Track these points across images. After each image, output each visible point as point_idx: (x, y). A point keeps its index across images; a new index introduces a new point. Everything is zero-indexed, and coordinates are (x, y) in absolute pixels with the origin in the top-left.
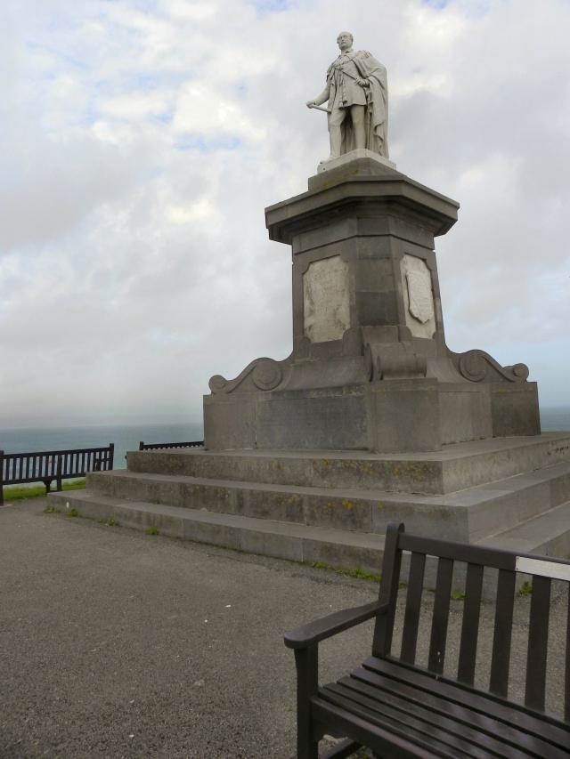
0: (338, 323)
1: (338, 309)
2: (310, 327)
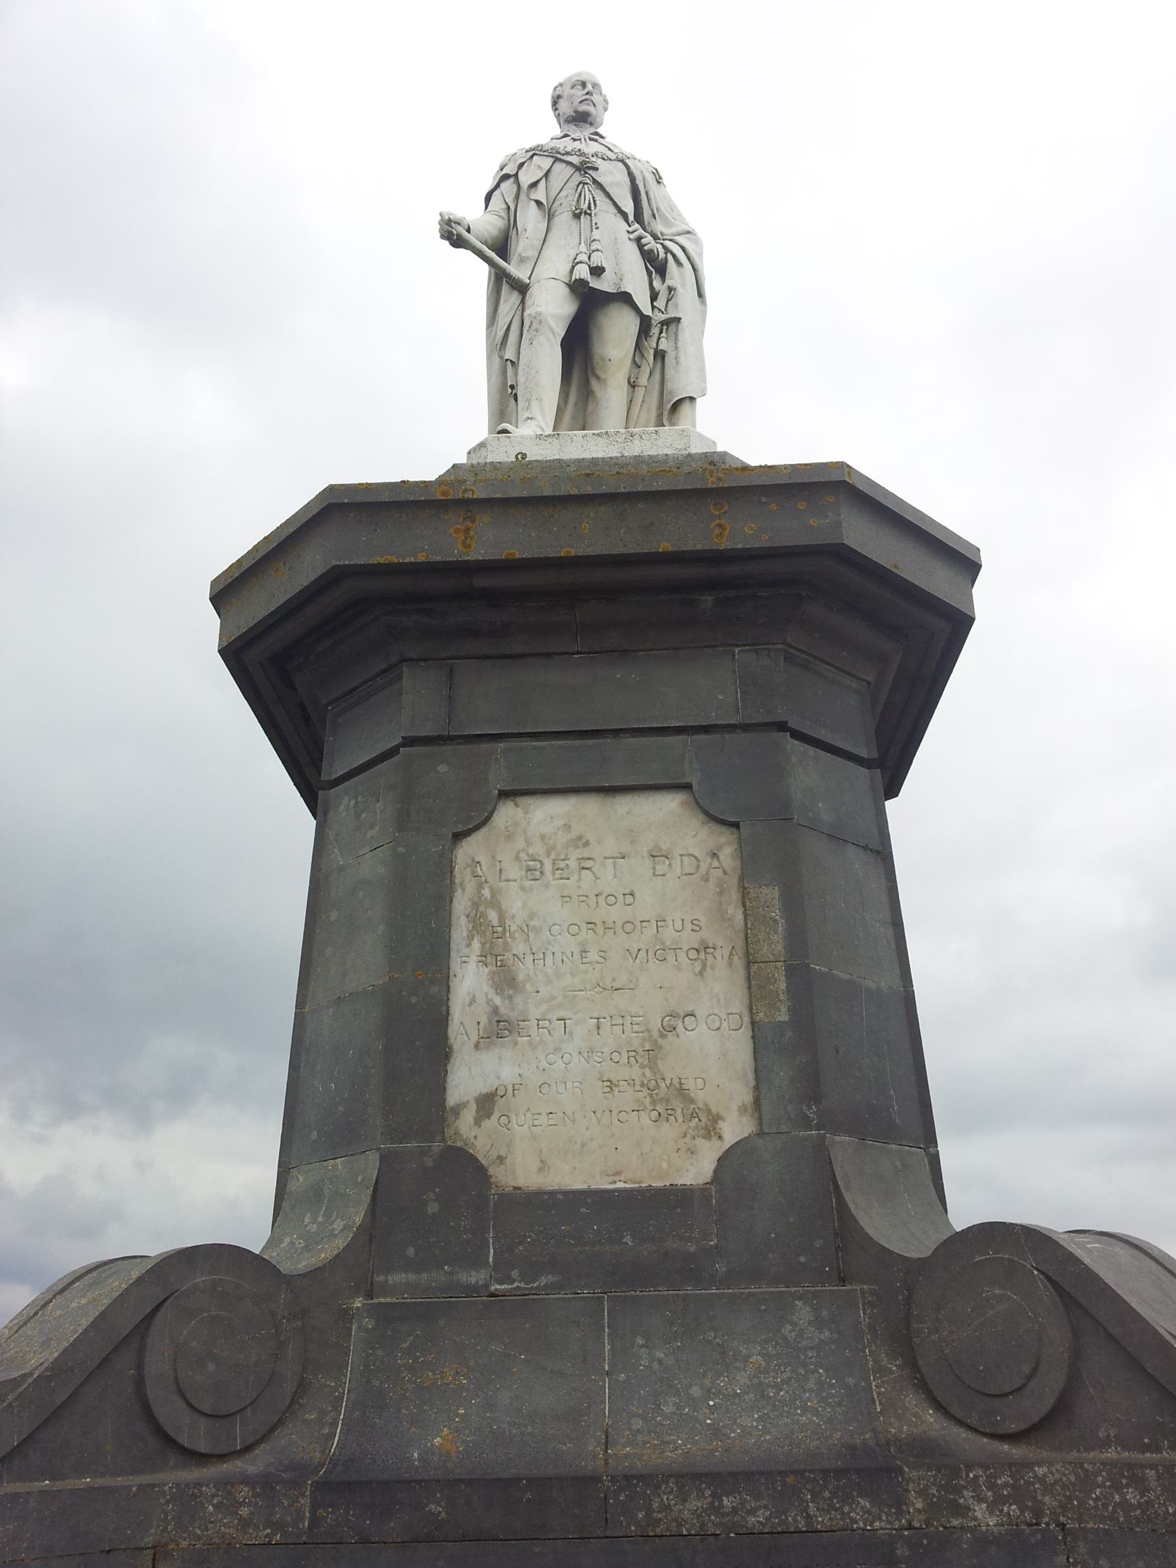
0: (673, 1101)
1: (668, 1030)
2: (487, 1103)
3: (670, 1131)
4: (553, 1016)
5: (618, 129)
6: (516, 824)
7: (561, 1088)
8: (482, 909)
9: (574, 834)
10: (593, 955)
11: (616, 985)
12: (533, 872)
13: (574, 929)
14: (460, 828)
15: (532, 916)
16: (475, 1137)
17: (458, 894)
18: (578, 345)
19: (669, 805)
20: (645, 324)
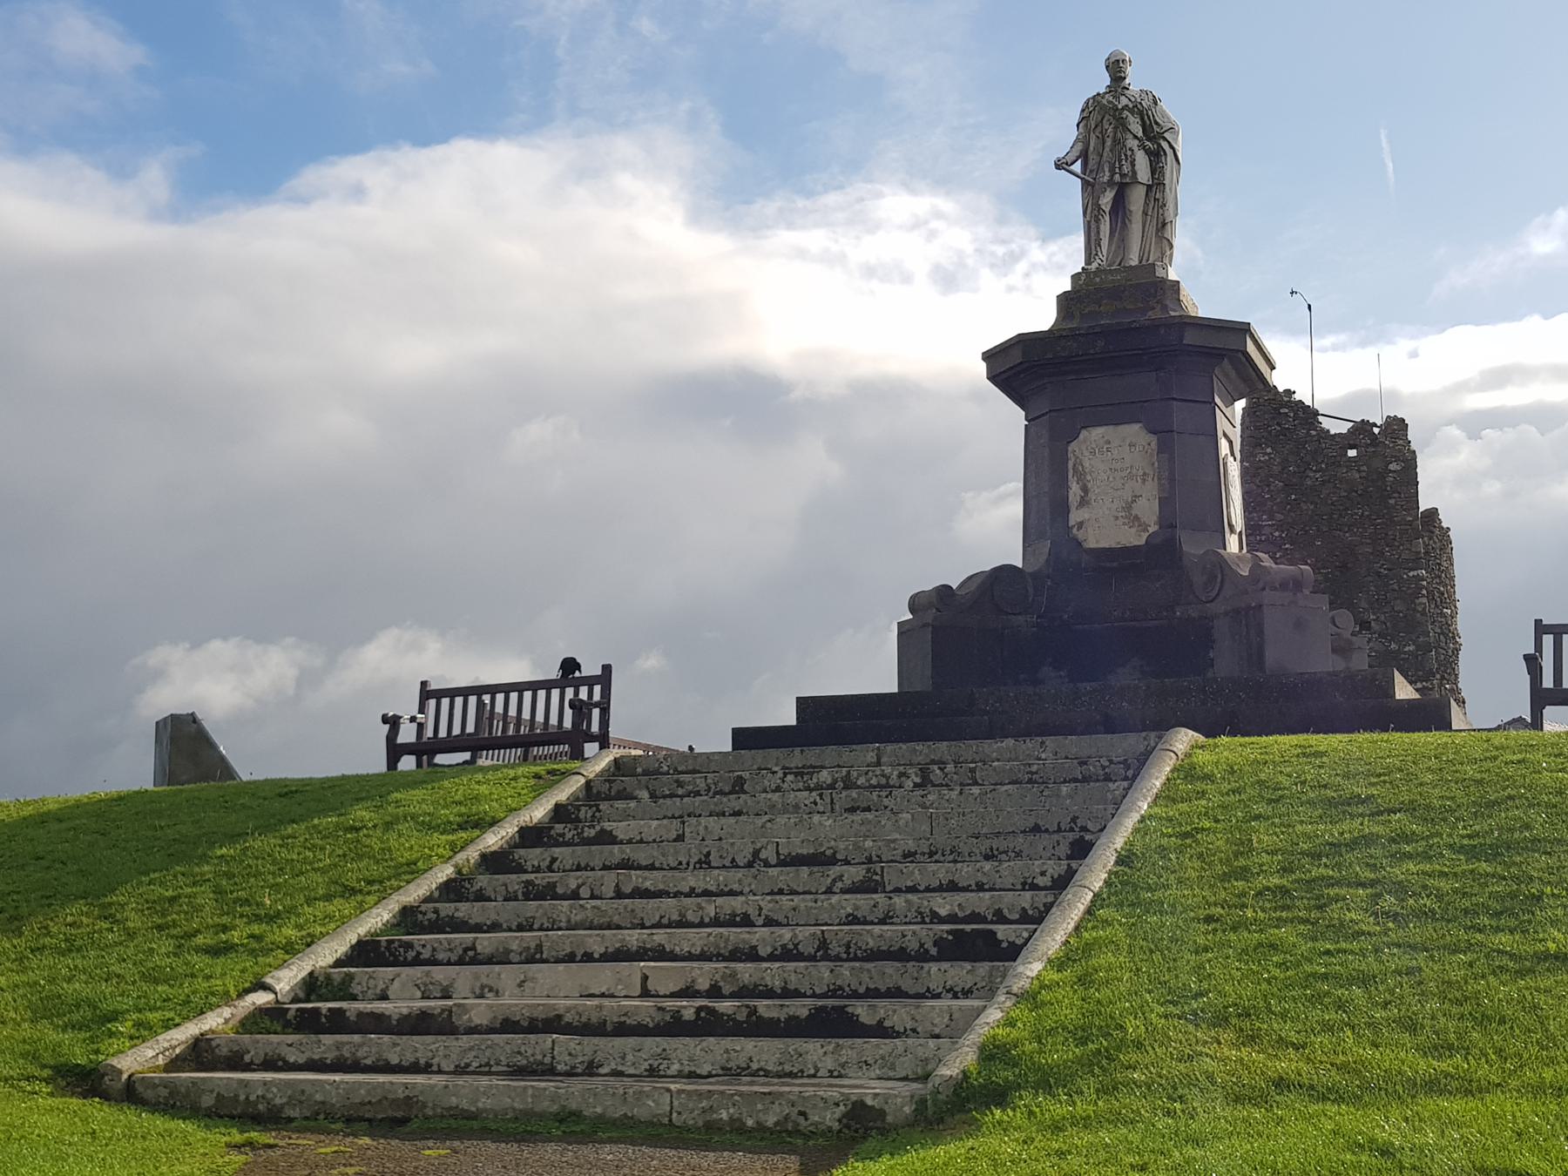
2: (1080, 525)
3: (1133, 530)
5: (1136, 81)
18: (1119, 204)
19: (1136, 427)
20: (1149, 187)
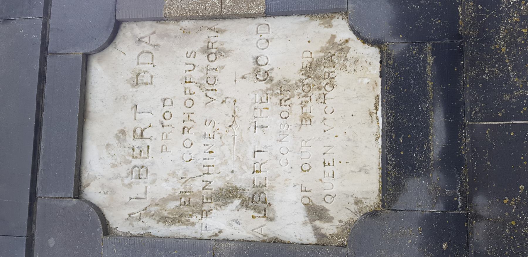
1: (267, 77)
2: (316, 213)
3: (341, 77)
4: (252, 161)
6: (102, 186)
7: (305, 155)
8: (166, 214)
9: (114, 142)
10: (208, 130)
11: (232, 113)
12: (140, 173)
13: (187, 143)
14: (100, 229)
15: (174, 174)
16: (340, 221)
17: (154, 232)
19: (100, 72)
